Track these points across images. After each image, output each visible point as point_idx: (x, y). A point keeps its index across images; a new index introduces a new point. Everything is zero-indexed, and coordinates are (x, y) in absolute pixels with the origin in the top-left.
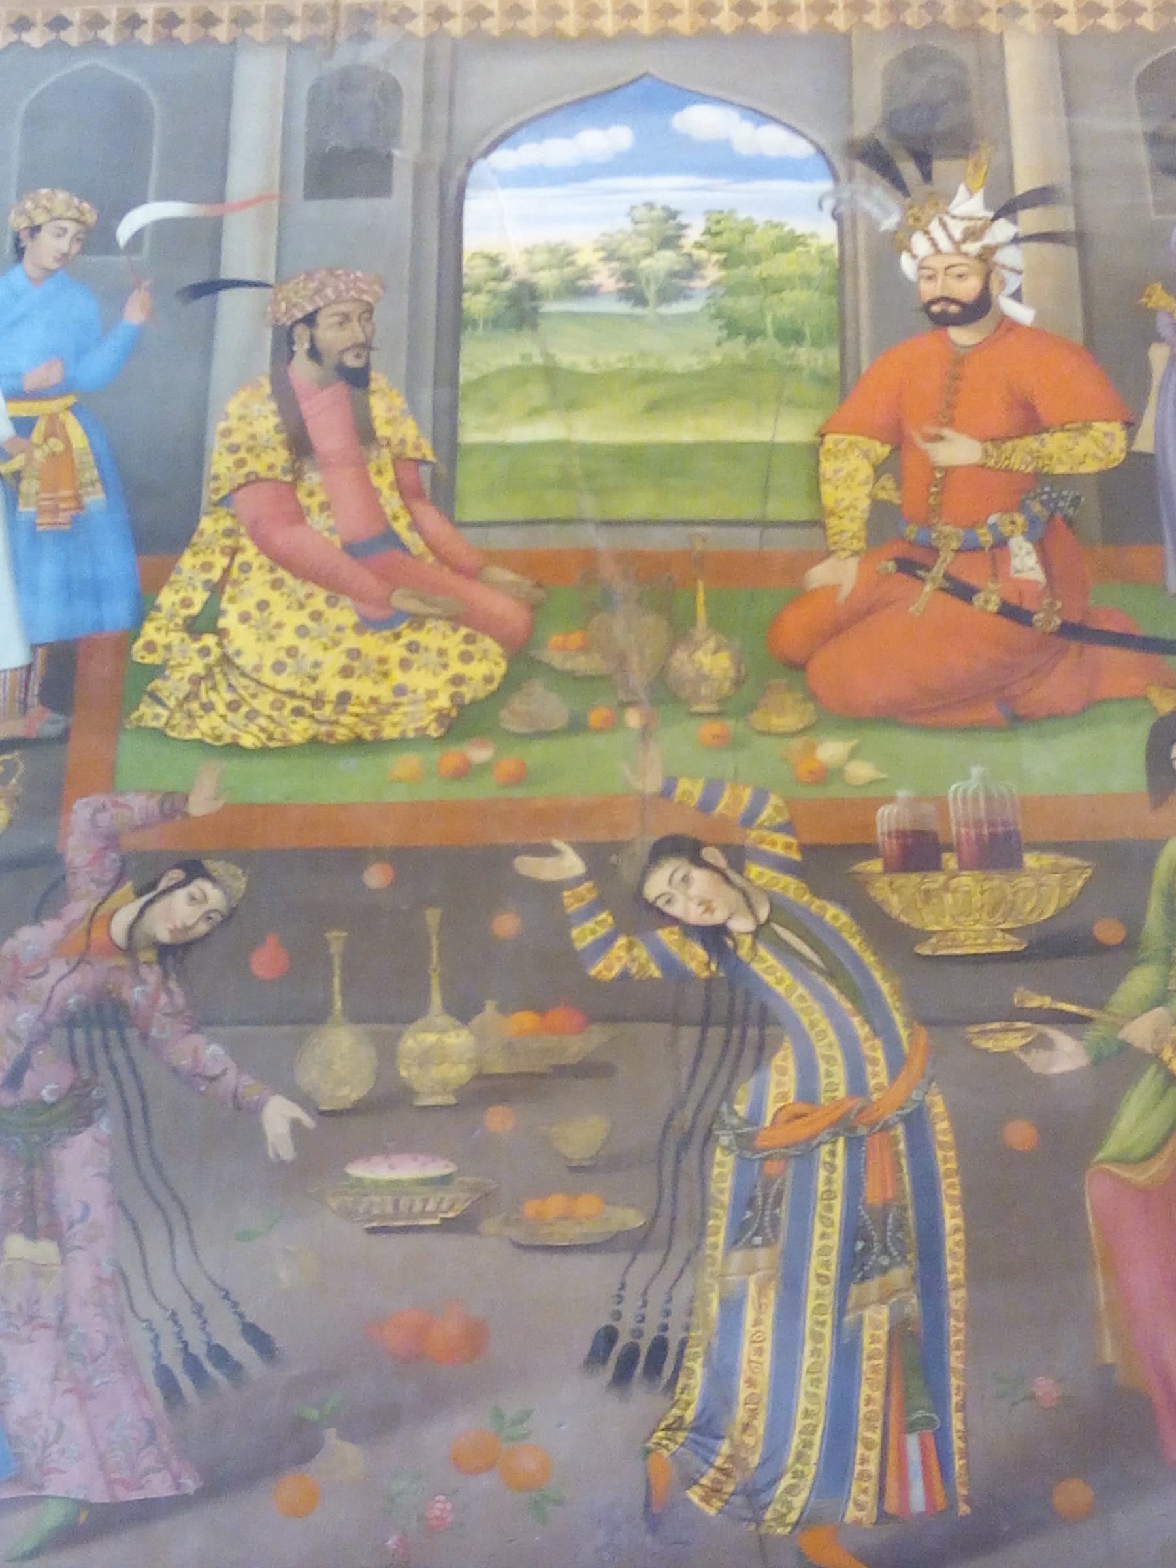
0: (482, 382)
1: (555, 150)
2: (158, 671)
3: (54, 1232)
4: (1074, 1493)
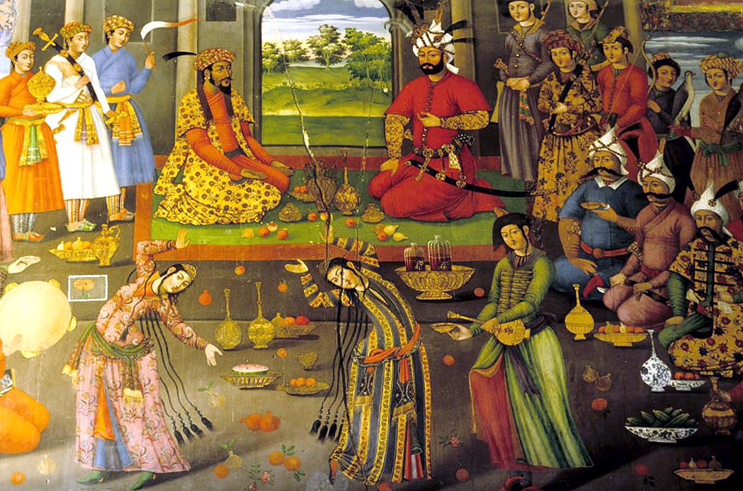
0: (270, 92)
2: (164, 197)
3: (140, 388)
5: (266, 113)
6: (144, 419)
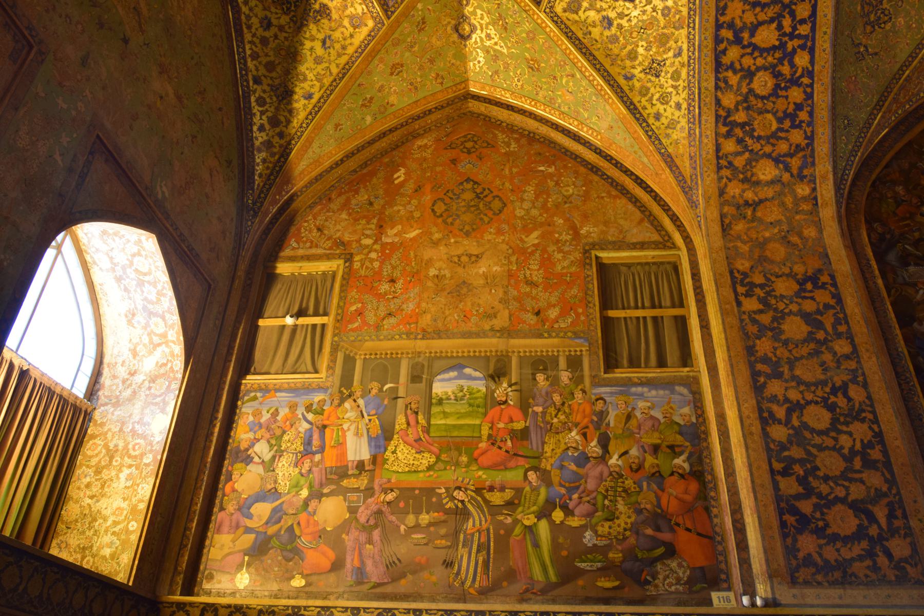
1: (446, 376)
4: (505, 584)
5: (432, 423)
6: (373, 558)
